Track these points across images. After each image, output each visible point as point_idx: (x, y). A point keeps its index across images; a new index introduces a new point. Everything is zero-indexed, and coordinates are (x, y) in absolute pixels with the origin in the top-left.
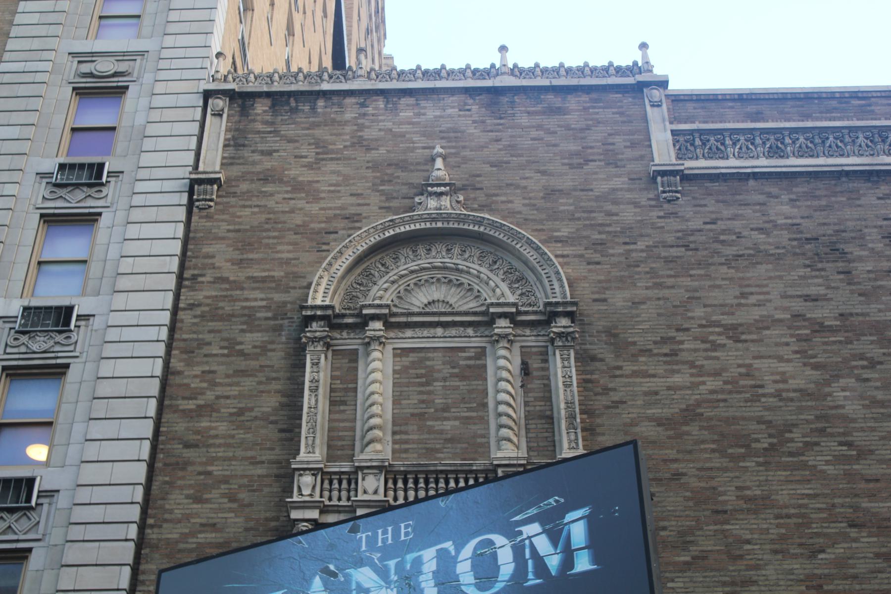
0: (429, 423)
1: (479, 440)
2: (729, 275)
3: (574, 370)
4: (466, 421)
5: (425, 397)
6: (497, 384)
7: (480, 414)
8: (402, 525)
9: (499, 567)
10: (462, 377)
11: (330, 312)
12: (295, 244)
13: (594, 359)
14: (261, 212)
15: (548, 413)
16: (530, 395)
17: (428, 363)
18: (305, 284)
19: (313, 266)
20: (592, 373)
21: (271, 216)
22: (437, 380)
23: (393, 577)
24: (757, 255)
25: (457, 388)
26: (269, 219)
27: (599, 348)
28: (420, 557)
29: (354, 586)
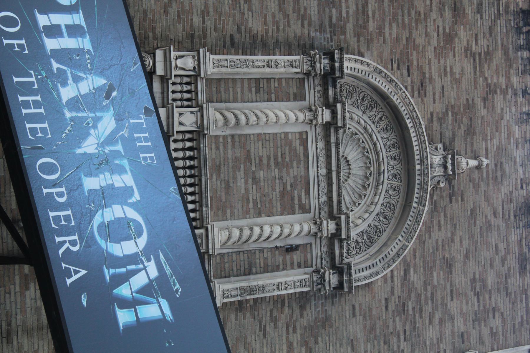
3: (292, 291)
5: (265, 161)
6: (278, 224)
7: (252, 211)
8: (153, 155)
9: (118, 242)
10: (283, 194)
11: (337, 74)
13: (302, 308)
16: (269, 254)
17: (295, 163)
18: (362, 50)
19: (378, 56)
22: (280, 171)
23: (107, 149)
25: (274, 190)
26: (420, 14)
27: (312, 312)
28: (126, 172)
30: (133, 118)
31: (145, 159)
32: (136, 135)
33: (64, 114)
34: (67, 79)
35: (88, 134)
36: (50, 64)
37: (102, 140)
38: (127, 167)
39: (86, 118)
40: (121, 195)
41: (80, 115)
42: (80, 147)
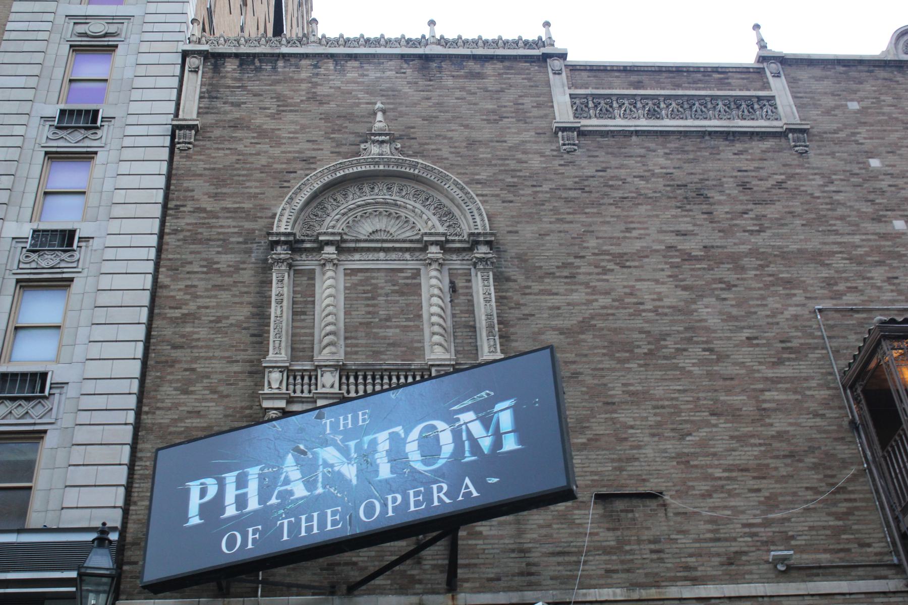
0: (374, 330)
1: (416, 345)
2: (617, 214)
3: (492, 288)
4: (405, 329)
5: (371, 309)
6: (430, 299)
8: (360, 413)
9: (440, 448)
10: (402, 294)
11: (291, 238)
12: (261, 181)
13: (508, 279)
14: (231, 154)
15: (472, 323)
17: (373, 281)
18: (270, 215)
20: (507, 291)
21: (240, 157)
22: (380, 295)
23: (354, 455)
24: (639, 198)
27: (512, 271)
28: (375, 438)
29: (321, 462)
30: (325, 430)
31: (364, 420)
32: (342, 428)
33: (319, 495)
34: (286, 490)
35: (339, 472)
36: (271, 505)
37: (345, 460)
38: (371, 437)
39: (324, 474)
40: (397, 443)
41: (320, 479)
42: (351, 481)
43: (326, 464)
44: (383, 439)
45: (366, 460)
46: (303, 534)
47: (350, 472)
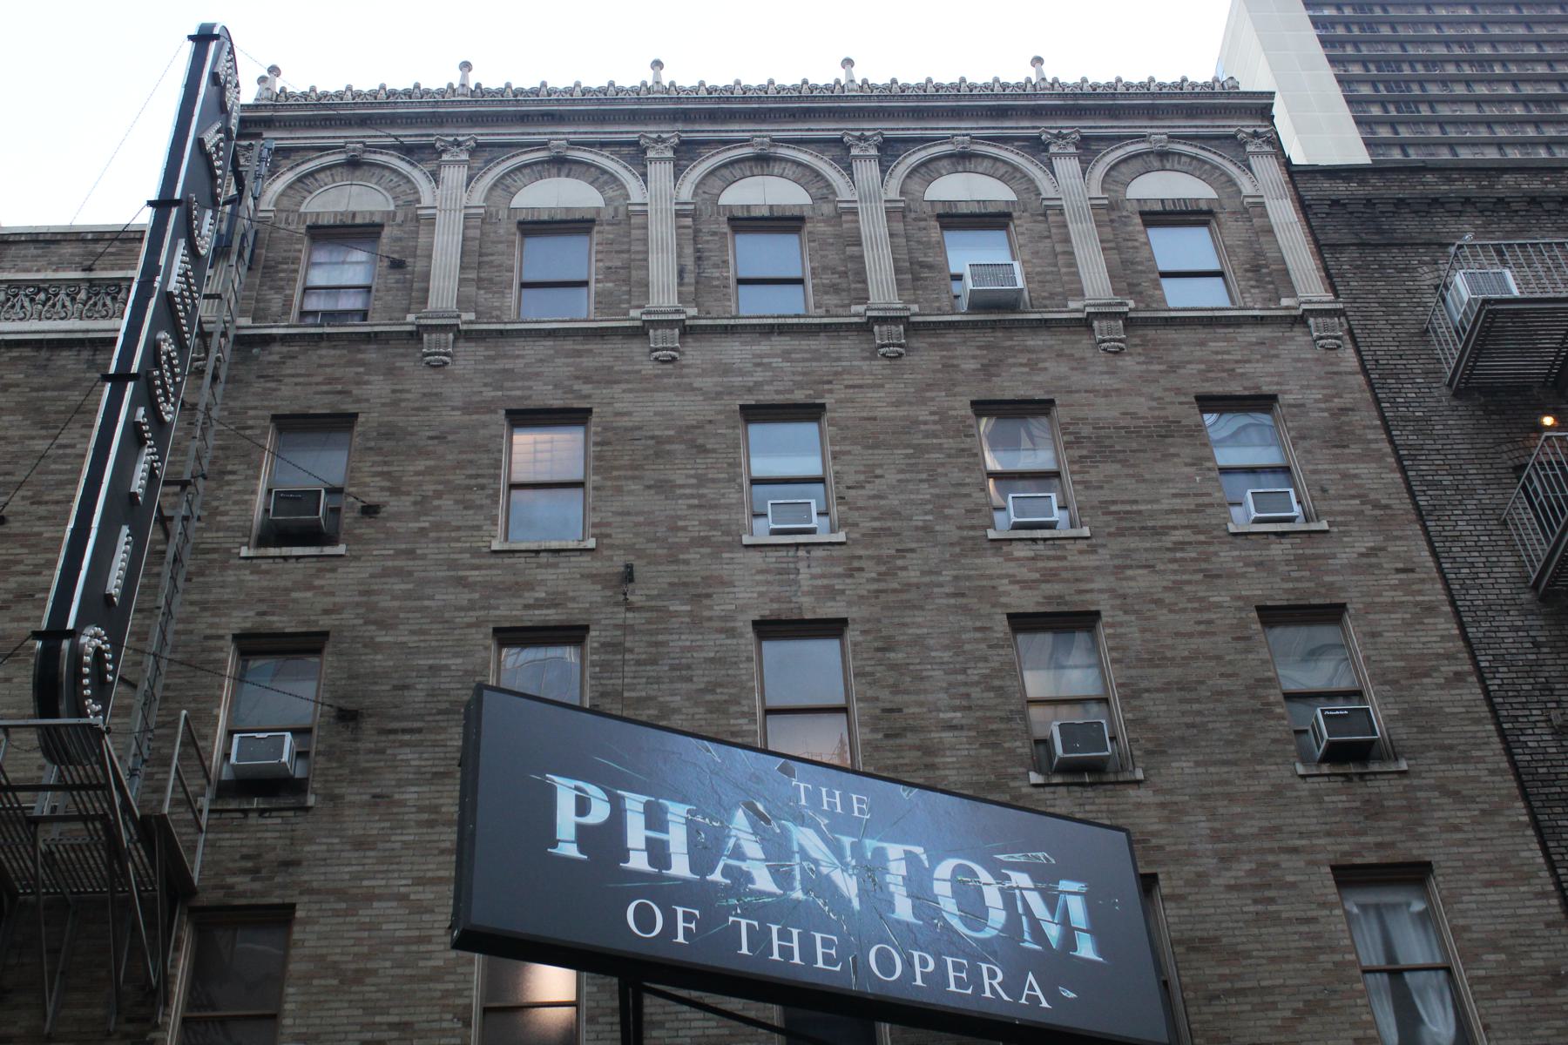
28: (883, 849)
29: (796, 848)
30: (798, 799)
31: (861, 811)
32: (825, 807)
33: (799, 901)
35: (828, 877)
39: (802, 869)
41: (798, 877)
42: (850, 901)
43: (805, 855)
44: (895, 851)
45: (871, 872)
46: (776, 956)
47: (848, 885)
